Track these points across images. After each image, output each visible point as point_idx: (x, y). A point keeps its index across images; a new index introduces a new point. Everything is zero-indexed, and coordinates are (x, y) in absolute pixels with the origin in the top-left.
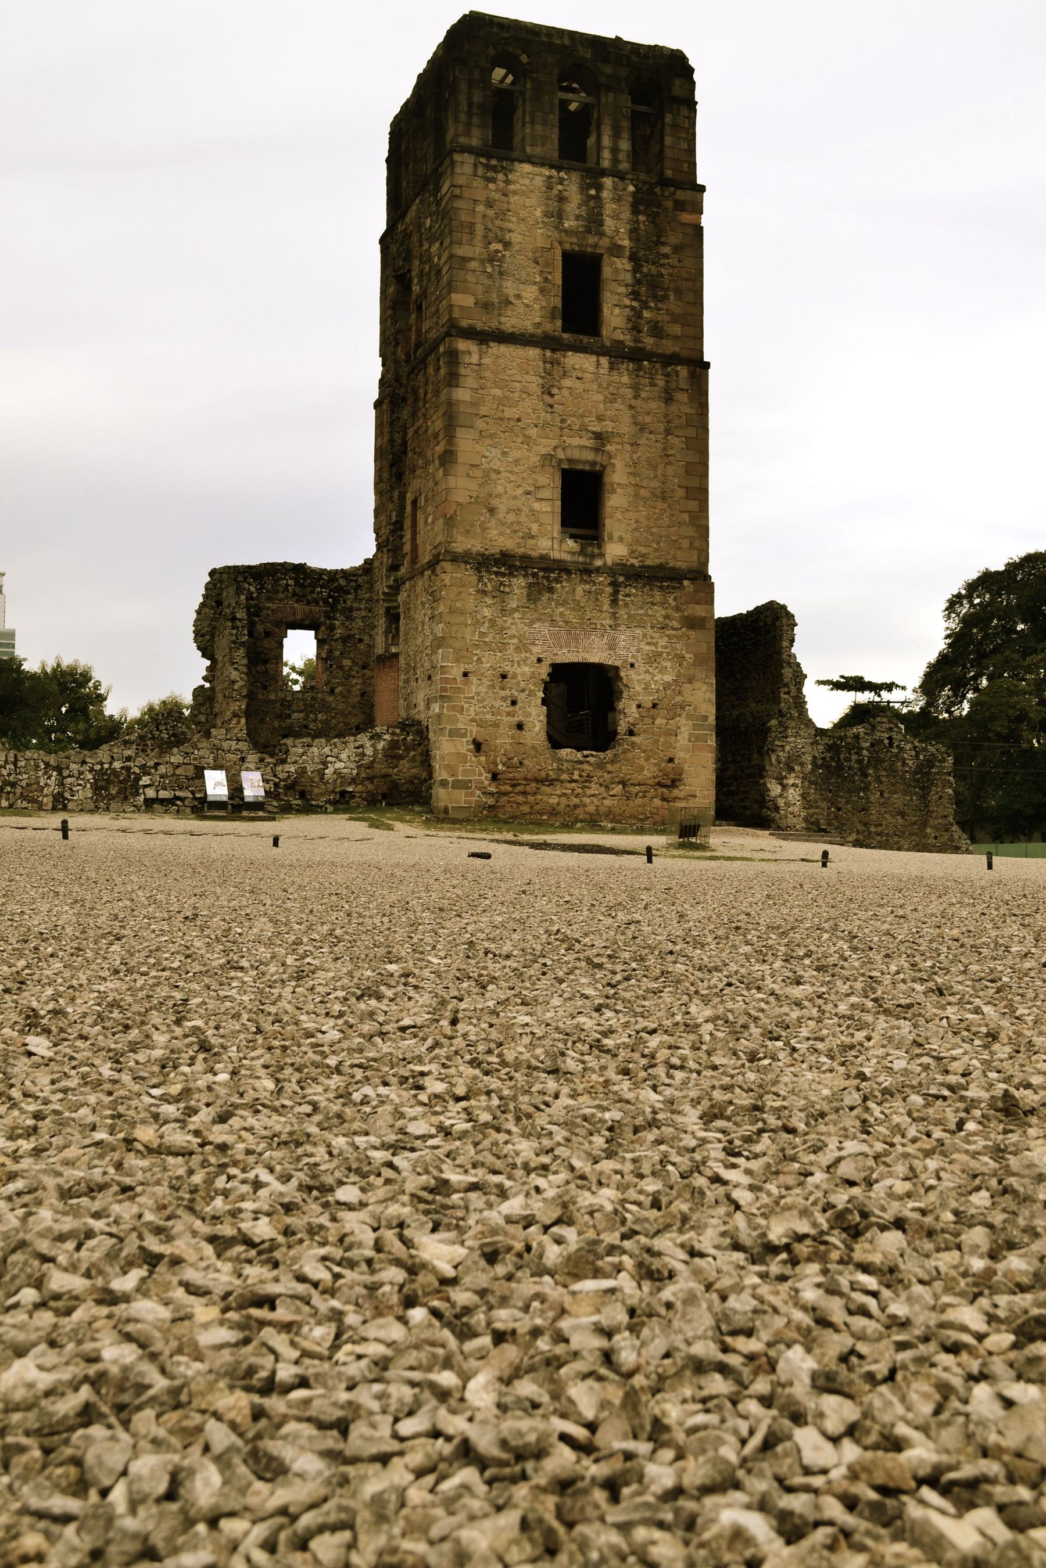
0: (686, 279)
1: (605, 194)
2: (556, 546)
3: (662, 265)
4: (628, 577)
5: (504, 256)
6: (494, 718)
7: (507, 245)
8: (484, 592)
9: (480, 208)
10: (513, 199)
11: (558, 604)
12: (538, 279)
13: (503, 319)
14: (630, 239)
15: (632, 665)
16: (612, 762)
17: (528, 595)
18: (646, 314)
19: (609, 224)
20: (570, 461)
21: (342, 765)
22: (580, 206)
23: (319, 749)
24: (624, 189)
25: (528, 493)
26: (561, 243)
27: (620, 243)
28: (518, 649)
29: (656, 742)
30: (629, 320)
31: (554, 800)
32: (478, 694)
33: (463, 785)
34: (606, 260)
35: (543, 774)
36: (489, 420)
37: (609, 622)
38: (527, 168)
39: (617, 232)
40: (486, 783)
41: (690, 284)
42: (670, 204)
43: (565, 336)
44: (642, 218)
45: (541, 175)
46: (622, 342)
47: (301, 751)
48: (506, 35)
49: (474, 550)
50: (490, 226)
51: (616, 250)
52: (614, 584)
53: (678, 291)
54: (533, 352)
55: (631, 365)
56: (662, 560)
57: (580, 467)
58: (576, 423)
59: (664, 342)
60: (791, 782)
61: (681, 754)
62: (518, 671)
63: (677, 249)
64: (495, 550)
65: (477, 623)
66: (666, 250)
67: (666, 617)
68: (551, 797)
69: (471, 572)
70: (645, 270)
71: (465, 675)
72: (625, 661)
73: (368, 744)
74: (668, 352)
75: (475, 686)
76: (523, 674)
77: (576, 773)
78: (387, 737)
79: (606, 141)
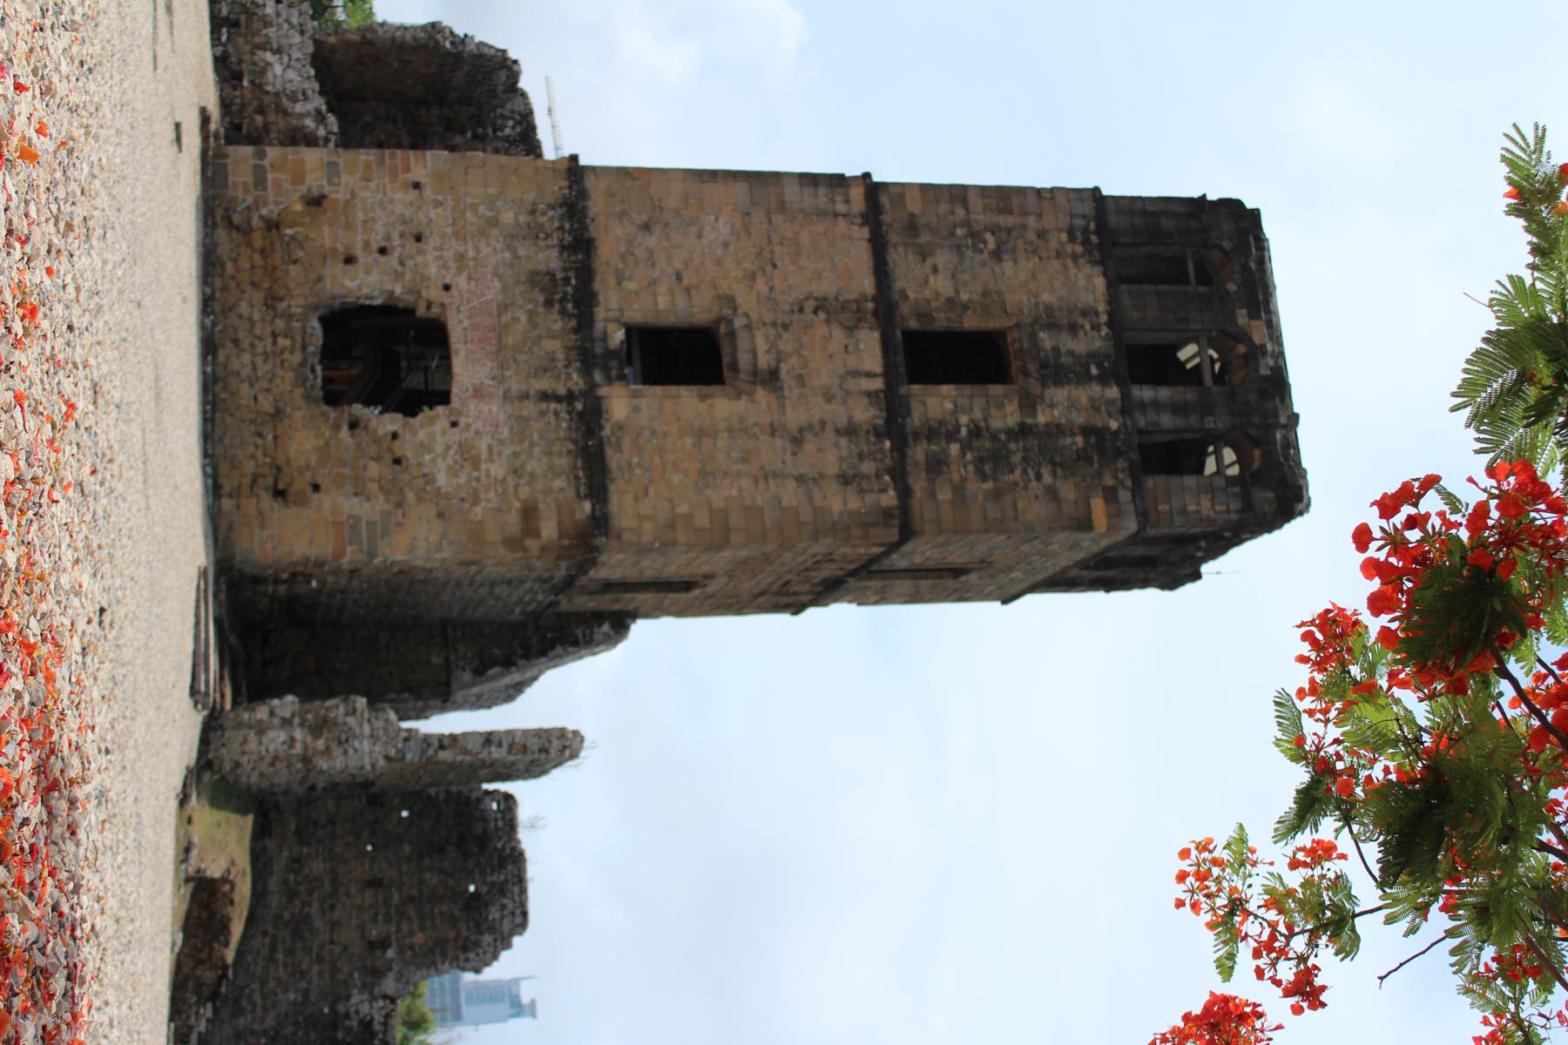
0: (1015, 506)
1: (1096, 389)
2: (611, 314)
3: (1025, 472)
4: (581, 415)
5: (981, 251)
6: (359, 223)
7: (997, 255)
8: (533, 212)
9: (1032, 221)
10: (1055, 264)
11: (532, 315)
12: (964, 297)
13: (901, 249)
14: (1047, 425)
15: (454, 424)
16: (308, 397)
17: (538, 273)
18: (954, 449)
19: (1059, 394)
20: (732, 335)
21: (278, 69)
22: (1071, 353)
23: (300, 47)
24: (1110, 416)
25: (679, 277)
26: (1017, 326)
27: (1039, 408)
28: (461, 257)
29: (343, 463)
30: (941, 423)
31: (244, 308)
32: (392, 201)
33: (260, 181)
34: (1012, 388)
35: (282, 292)
36: (765, 226)
37: (515, 388)
38: (1100, 283)
39: (1052, 406)
40: (264, 212)
41: (1010, 512)
42: (1109, 481)
43: (898, 334)
44: (1080, 440)
45: (1095, 301)
46: (909, 413)
47: (295, 20)
48: (1253, 266)
49: (590, 203)
50: (1014, 234)
51: (1029, 404)
52: (570, 397)
53: (997, 495)
54: (868, 285)
55: (880, 422)
56: (615, 473)
57: (726, 349)
58: (787, 345)
59: (923, 475)
60: (298, 734)
61: (327, 504)
62: (430, 257)
63: (1052, 493)
64: (595, 230)
65: (491, 202)
66: (1047, 478)
67: (532, 475)
68: (250, 305)
69: (559, 195)
70: (1013, 446)
71: (417, 186)
72: (460, 413)
73: (310, 107)
74: (911, 480)
75: (402, 199)
76: (426, 265)
77: (288, 342)
78: (322, 132)
79: (1164, 393)
